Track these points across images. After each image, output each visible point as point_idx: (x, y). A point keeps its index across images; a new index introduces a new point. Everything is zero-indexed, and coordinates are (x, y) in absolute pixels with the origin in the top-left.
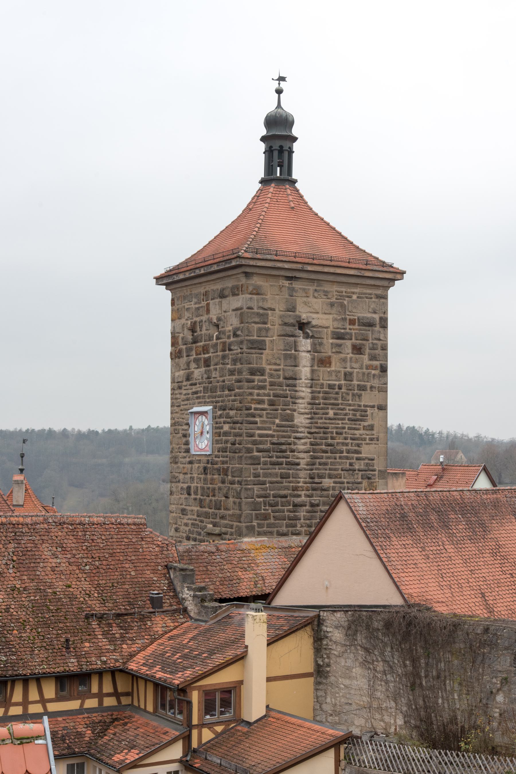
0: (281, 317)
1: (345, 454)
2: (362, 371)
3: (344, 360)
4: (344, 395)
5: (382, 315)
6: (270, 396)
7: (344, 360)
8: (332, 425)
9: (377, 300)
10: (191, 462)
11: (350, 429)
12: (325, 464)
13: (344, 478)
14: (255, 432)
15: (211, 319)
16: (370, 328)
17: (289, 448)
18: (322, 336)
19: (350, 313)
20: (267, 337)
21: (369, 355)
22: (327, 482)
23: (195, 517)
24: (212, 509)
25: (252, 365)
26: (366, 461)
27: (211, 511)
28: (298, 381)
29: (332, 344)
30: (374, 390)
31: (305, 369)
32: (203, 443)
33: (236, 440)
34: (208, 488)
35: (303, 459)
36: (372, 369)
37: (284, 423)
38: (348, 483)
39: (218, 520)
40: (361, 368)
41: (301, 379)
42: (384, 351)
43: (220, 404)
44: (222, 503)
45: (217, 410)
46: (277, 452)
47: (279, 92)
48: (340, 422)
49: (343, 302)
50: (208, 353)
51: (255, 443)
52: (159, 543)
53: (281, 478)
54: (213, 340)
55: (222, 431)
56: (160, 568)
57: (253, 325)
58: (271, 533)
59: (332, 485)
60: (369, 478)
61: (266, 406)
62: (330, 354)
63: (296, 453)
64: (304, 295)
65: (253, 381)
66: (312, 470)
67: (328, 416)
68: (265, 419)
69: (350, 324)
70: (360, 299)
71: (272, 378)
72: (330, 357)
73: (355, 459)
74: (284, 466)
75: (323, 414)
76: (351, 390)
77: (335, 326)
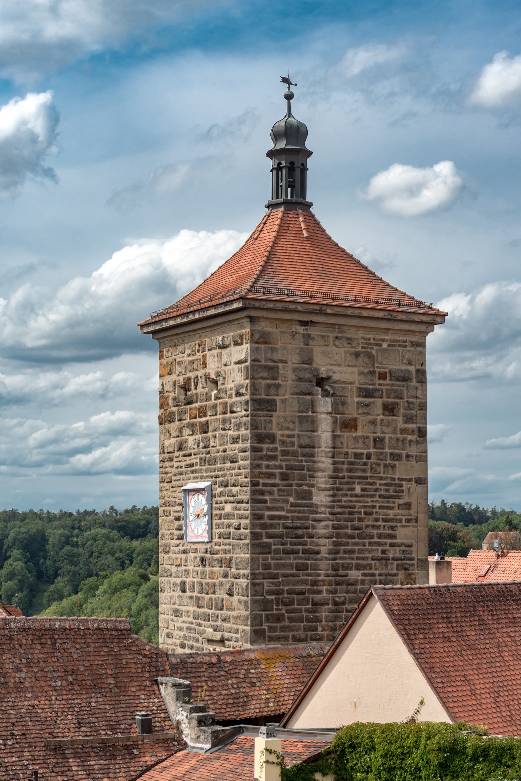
0: (295, 370)
1: (376, 540)
2: (396, 436)
3: (373, 423)
4: (374, 466)
5: (420, 367)
6: (282, 468)
7: (373, 423)
8: (360, 504)
9: (412, 349)
10: (185, 552)
11: (381, 507)
12: (352, 552)
13: (376, 569)
14: (264, 514)
15: (209, 374)
16: (404, 383)
17: (307, 533)
18: (346, 394)
19: (380, 365)
20: (277, 395)
21: (404, 415)
22: (354, 574)
23: (191, 619)
24: (212, 609)
25: (259, 431)
26: (403, 548)
27: (210, 612)
28: (316, 450)
29: (358, 403)
30: (410, 459)
31: (325, 434)
32: (200, 528)
33: (240, 525)
34: (207, 584)
35: (324, 546)
36: (408, 434)
37: (299, 501)
38: (380, 575)
39: (219, 623)
40: (394, 432)
41: (320, 447)
42: (422, 412)
43: (221, 479)
44: (224, 602)
45: (217, 486)
46: (292, 538)
47: (289, 97)
48: (369, 500)
49: (371, 352)
50: (205, 416)
51: (264, 526)
52: (148, 653)
53: (297, 570)
54: (211, 400)
55: (223, 512)
56: (148, 683)
57: (260, 380)
58: (286, 638)
59: (361, 578)
60: (406, 569)
61: (277, 481)
62: (356, 416)
63: (315, 539)
64: (322, 343)
65: (261, 450)
66: (335, 559)
67: (353, 492)
68: (277, 497)
69: (379, 379)
70: (392, 348)
71: (284, 446)
72: (355, 420)
73: (388, 545)
74: (301, 555)
75: (348, 490)
76: (382, 460)
77: (361, 381)
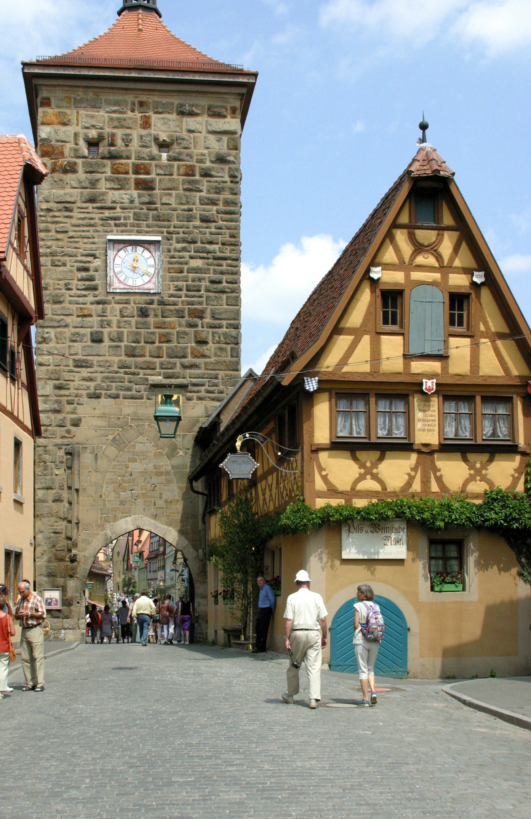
24: (162, 357)
27: (157, 360)
55: (186, 267)
